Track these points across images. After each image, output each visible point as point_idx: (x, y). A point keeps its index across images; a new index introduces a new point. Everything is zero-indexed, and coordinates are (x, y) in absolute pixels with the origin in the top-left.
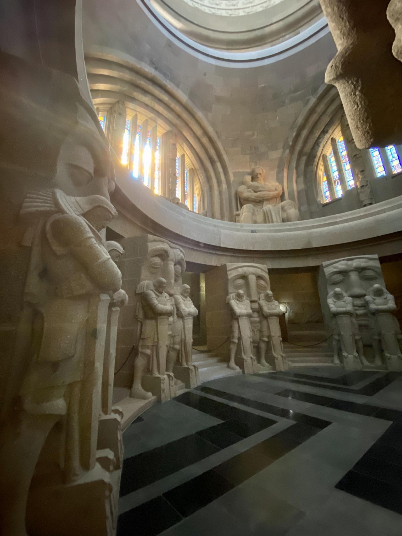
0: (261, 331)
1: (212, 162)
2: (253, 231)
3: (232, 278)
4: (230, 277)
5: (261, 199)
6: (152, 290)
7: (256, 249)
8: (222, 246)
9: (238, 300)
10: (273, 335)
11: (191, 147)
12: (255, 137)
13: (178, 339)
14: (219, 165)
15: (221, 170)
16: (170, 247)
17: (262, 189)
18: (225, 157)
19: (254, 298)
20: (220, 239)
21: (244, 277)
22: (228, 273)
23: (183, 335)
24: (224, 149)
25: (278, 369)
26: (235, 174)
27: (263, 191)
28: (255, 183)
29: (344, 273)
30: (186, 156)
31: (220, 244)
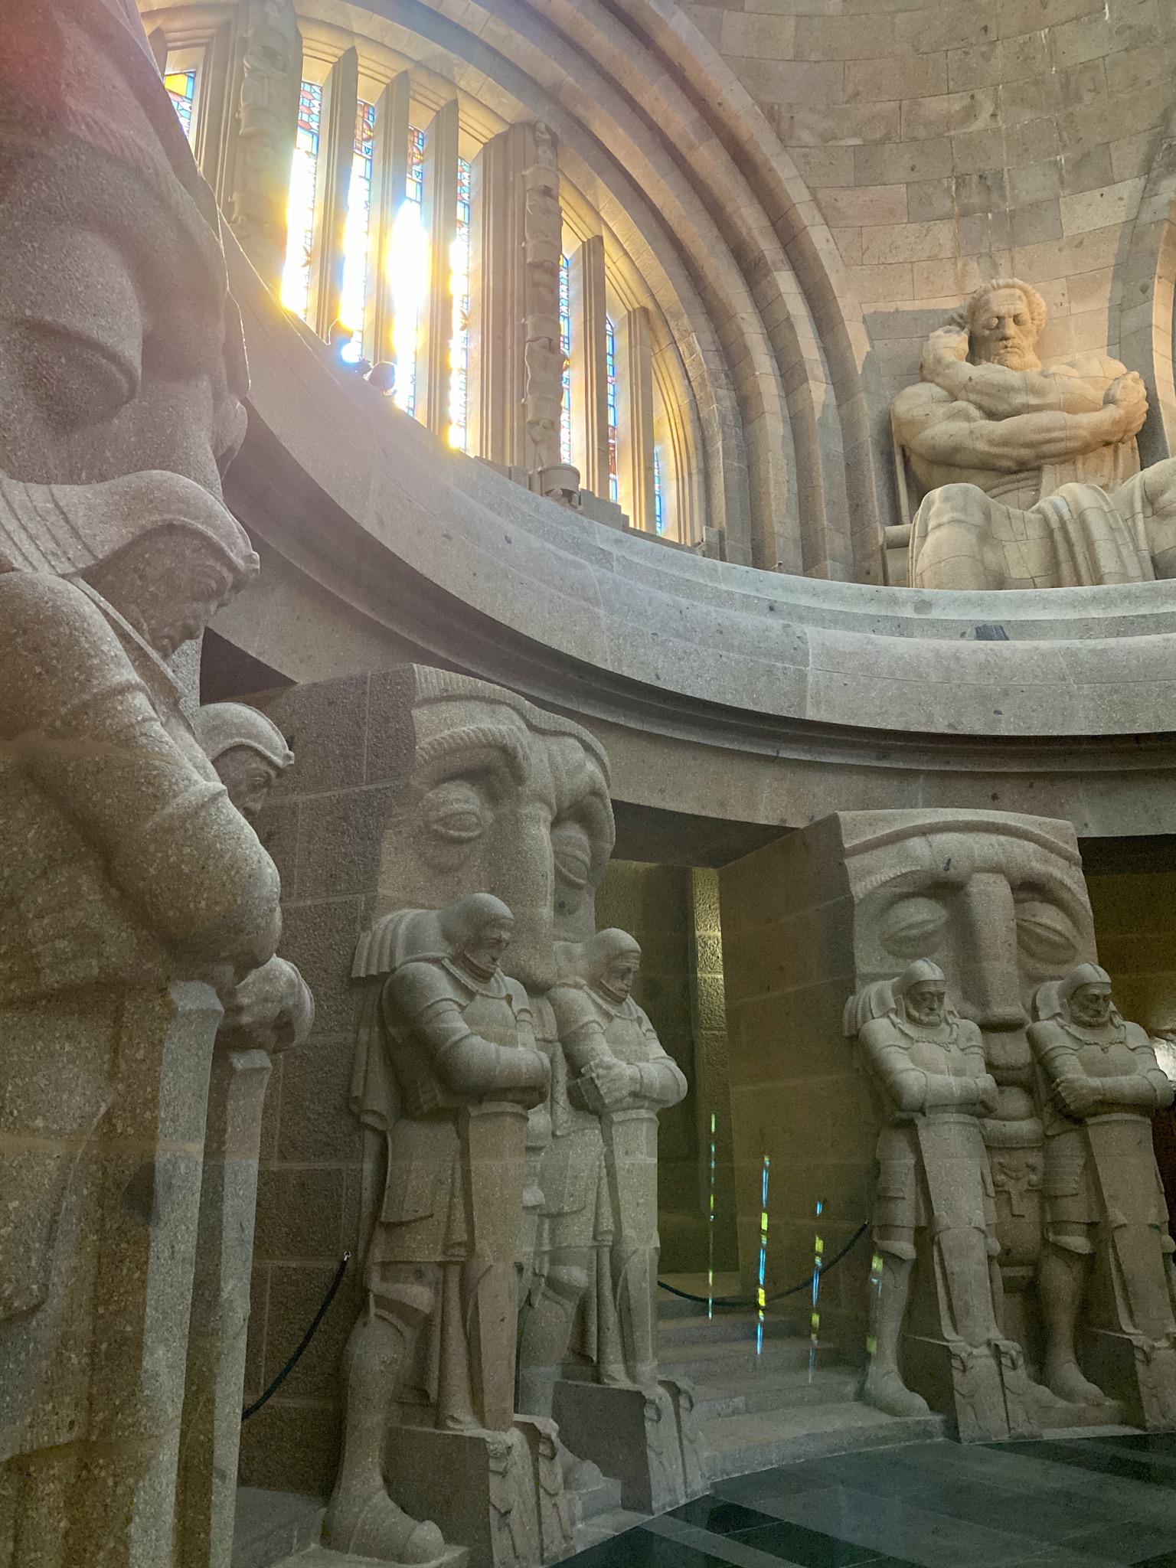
0: (1046, 1197)
1: (751, 270)
2: (984, 632)
3: (870, 896)
4: (859, 889)
5: (1025, 453)
6: (436, 961)
7: (1003, 730)
8: (811, 714)
9: (910, 1018)
10: (1122, 1219)
11: (633, 194)
12: (982, 122)
13: (578, 1234)
14: (786, 282)
15: (795, 306)
16: (532, 728)
17: (1033, 401)
18: (819, 237)
19: (1002, 1010)
20: (802, 677)
21: (945, 888)
22: (852, 863)
23: (606, 1211)
24: (815, 199)
25: (1154, 1420)
26: (876, 325)
27: (1038, 408)
28: (987, 372)
30: (608, 245)
31: (802, 707)
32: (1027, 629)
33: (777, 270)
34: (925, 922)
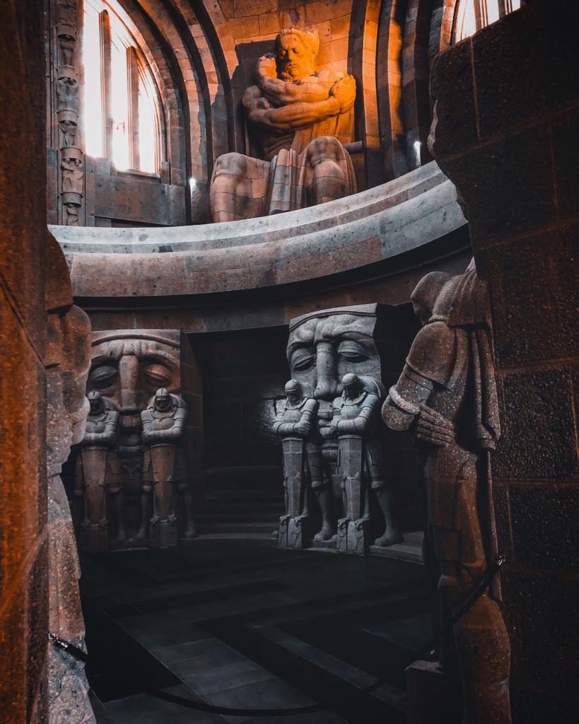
2: (163, 249)
5: (286, 126)
14: (196, 30)
15: (202, 44)
26: (242, 50)
29: (310, 345)
32: (180, 247)
33: (191, 24)
34: (106, 375)
